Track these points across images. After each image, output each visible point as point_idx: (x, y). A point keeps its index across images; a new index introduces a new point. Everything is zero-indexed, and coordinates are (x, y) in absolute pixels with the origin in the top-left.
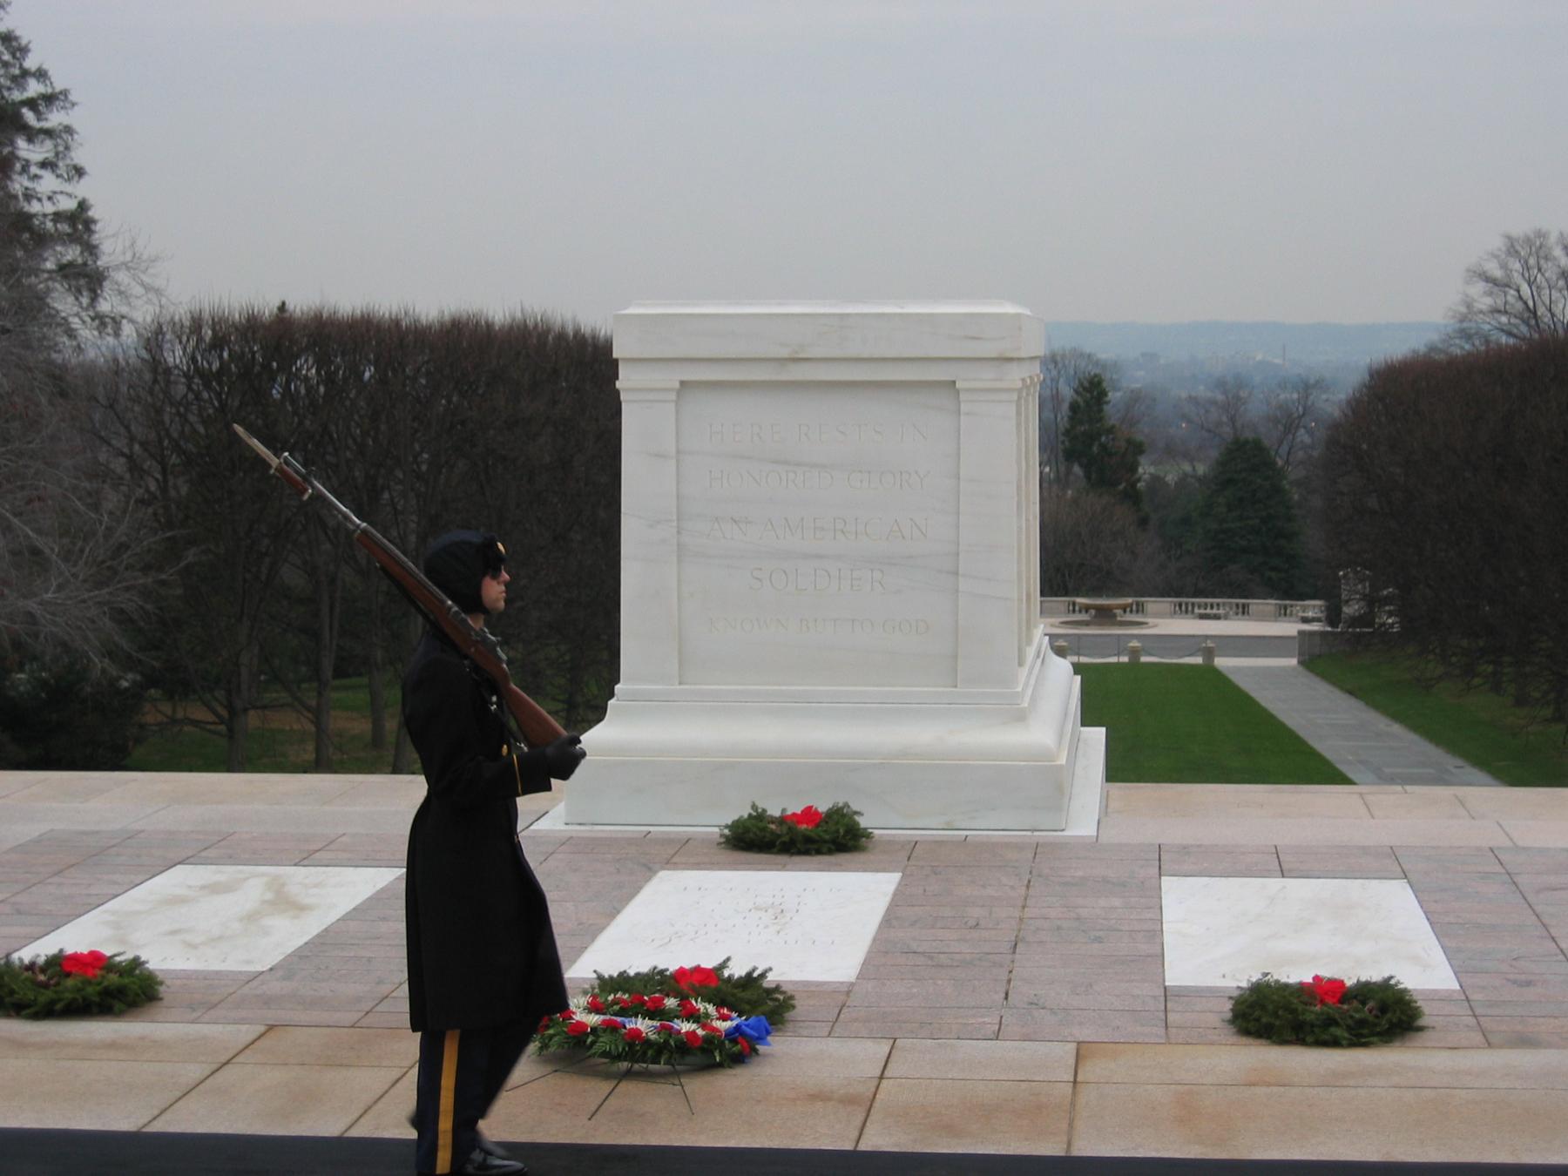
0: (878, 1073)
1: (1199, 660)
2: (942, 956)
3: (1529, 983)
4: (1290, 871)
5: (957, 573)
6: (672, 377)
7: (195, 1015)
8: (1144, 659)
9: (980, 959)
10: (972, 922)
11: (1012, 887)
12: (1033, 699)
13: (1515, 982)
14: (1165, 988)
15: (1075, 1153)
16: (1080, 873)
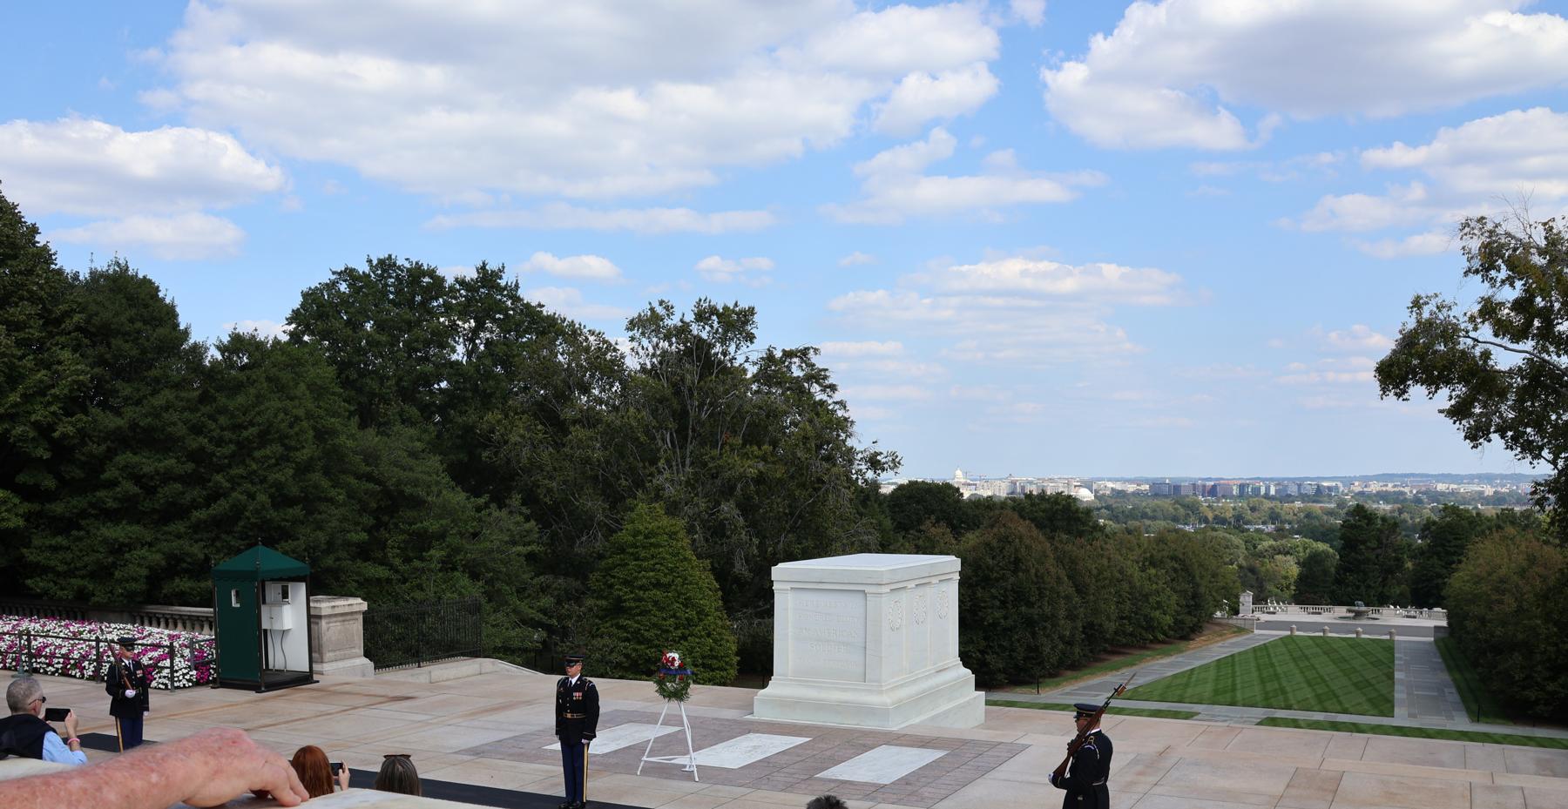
1: (1388, 637)
8: (1363, 636)
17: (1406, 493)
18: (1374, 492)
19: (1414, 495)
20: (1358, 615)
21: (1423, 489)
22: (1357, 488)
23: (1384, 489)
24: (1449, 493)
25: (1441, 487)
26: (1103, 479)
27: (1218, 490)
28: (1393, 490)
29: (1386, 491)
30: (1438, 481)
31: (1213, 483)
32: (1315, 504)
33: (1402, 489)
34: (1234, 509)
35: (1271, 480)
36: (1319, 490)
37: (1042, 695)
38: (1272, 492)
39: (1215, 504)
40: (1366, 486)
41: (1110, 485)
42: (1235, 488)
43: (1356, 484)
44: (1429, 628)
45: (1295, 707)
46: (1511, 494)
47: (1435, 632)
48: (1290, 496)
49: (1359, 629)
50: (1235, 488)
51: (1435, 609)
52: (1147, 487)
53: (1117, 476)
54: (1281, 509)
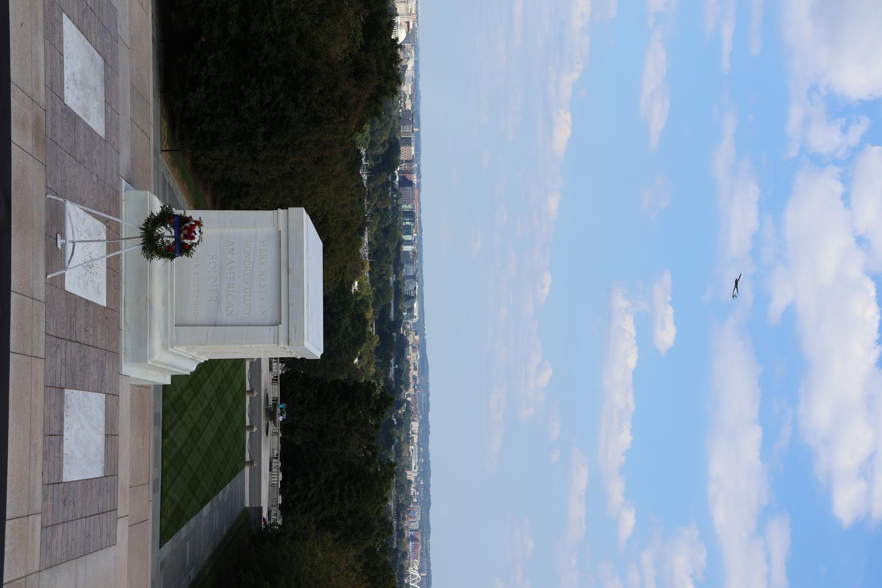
0: (34, 298)
1: (248, 459)
2: (75, 319)
3: (64, 504)
4: (108, 437)
5: (215, 326)
6: (282, 228)
7: (48, 84)
8: (248, 433)
9: (73, 331)
10: (87, 329)
11: (101, 343)
12: (173, 353)
13: (65, 500)
14: (63, 388)
15: (11, 354)
16: (107, 367)
17: (407, 390)
18: (408, 357)
19: (406, 400)
20: (271, 414)
21: (412, 408)
22: (412, 339)
23: (412, 367)
24: (408, 435)
25: (415, 426)
26: (417, 55)
27: (407, 188)
28: (411, 377)
29: (410, 370)
30: (421, 422)
31: (415, 181)
32: (393, 295)
33: (412, 386)
34: (386, 210)
35: (420, 246)
36: (410, 298)
37: (161, 156)
38: (406, 248)
39: (390, 189)
40: (414, 348)
41: (410, 64)
42: (410, 206)
43: (417, 338)
44: (260, 503)
45: (166, 440)
46: (409, 498)
47: (256, 508)
48: (402, 268)
49: (255, 429)
50: (410, 206)
51: (280, 474)
52: (409, 107)
53: (420, 69)
54: (386, 262)
